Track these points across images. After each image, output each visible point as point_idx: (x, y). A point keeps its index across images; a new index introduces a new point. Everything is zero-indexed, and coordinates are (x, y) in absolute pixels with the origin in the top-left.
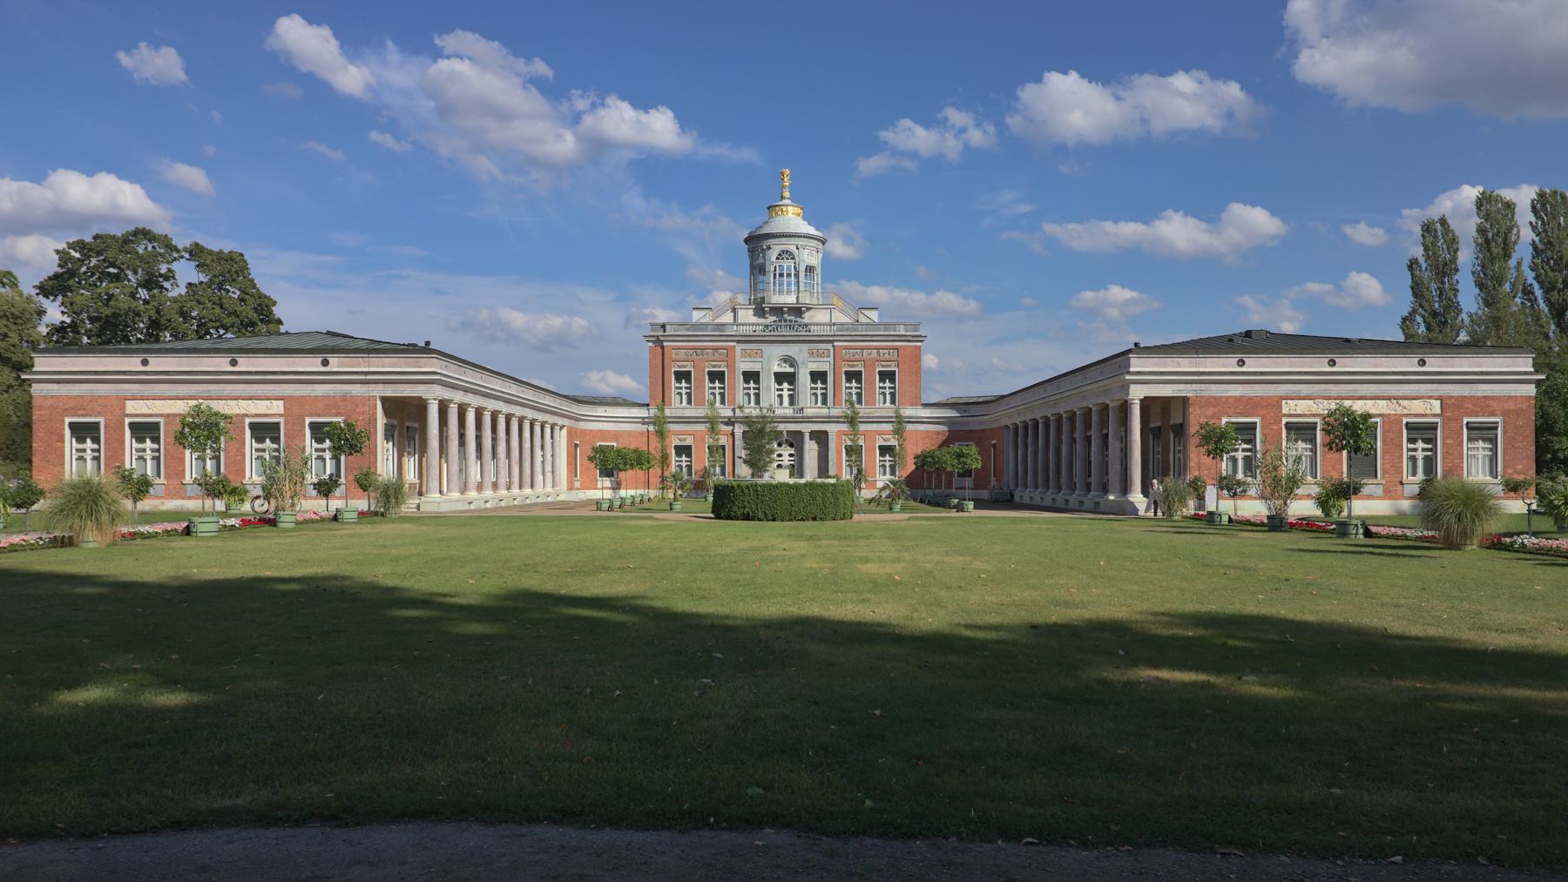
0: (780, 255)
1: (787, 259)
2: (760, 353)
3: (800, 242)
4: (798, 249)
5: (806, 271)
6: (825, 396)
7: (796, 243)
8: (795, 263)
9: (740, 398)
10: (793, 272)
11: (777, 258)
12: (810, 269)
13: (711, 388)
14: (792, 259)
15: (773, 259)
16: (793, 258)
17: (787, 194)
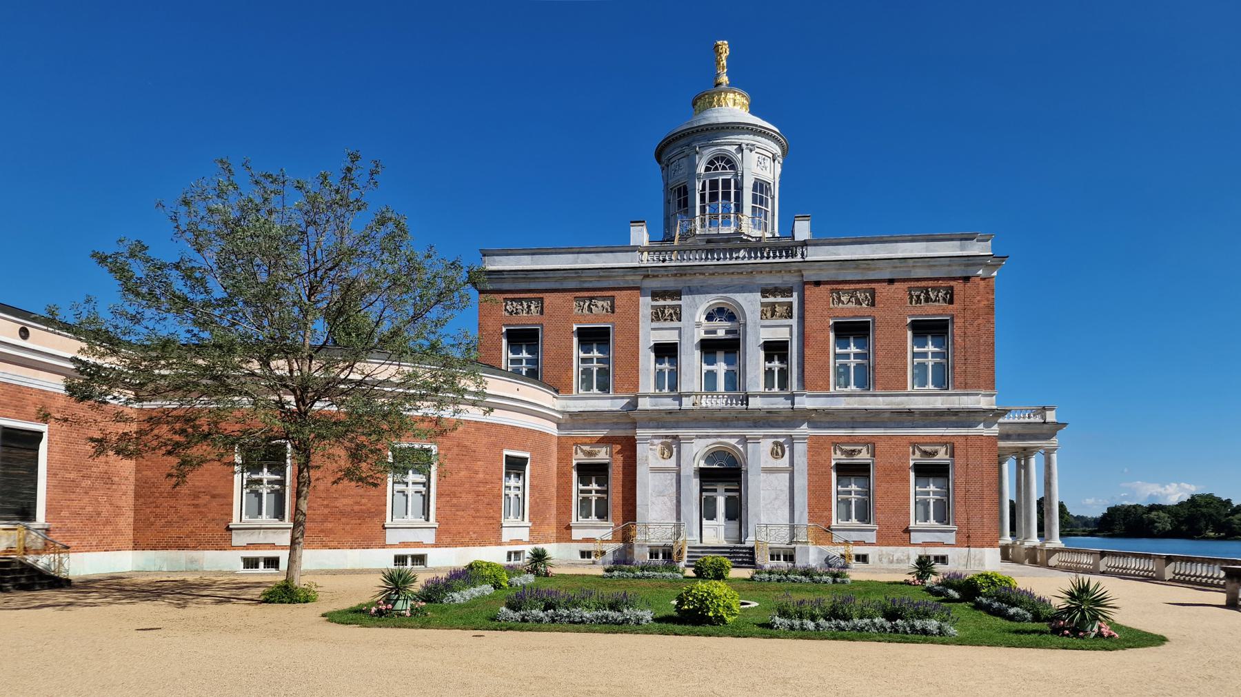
0: (711, 163)
1: (724, 168)
2: (677, 314)
3: (745, 139)
4: (740, 149)
5: (755, 188)
6: (784, 374)
7: (741, 141)
8: (737, 174)
9: (647, 384)
10: (733, 191)
11: (707, 169)
12: (761, 187)
13: (584, 360)
14: (731, 168)
15: (701, 169)
16: (733, 167)
17: (724, 79)
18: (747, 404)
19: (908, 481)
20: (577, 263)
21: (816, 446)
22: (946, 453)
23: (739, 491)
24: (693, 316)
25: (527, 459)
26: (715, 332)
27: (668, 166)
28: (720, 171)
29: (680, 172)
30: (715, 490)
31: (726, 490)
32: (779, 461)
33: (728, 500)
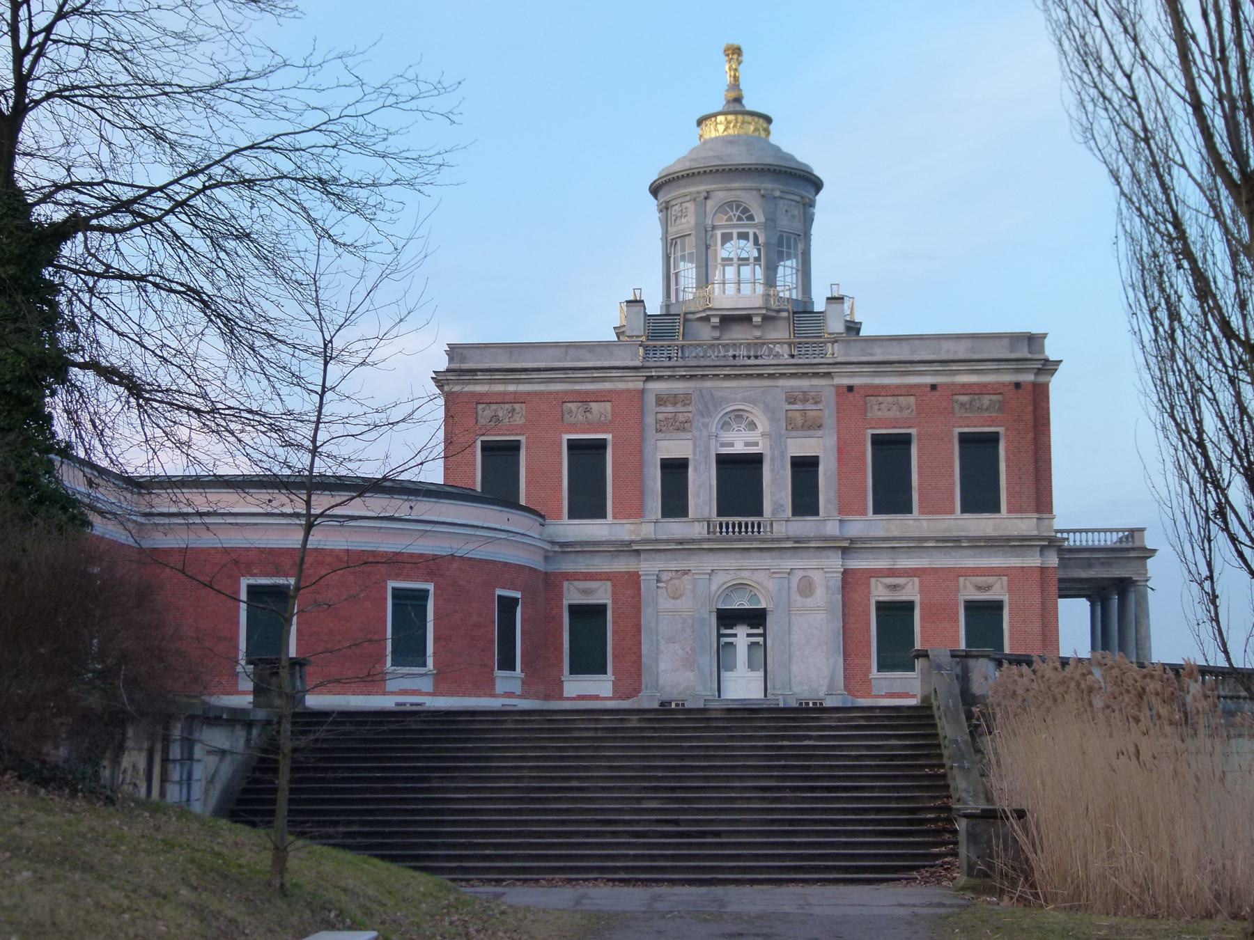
1: (740, 219)
18: (772, 532)
19: (957, 621)
20: (565, 360)
21: (850, 581)
22: (1002, 587)
23: (764, 635)
24: (706, 425)
25: (518, 599)
26: (732, 445)
27: (667, 209)
28: (735, 222)
29: (684, 220)
30: (735, 635)
31: (749, 635)
32: (809, 600)
33: (752, 645)
